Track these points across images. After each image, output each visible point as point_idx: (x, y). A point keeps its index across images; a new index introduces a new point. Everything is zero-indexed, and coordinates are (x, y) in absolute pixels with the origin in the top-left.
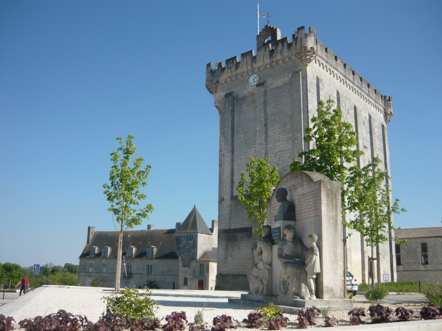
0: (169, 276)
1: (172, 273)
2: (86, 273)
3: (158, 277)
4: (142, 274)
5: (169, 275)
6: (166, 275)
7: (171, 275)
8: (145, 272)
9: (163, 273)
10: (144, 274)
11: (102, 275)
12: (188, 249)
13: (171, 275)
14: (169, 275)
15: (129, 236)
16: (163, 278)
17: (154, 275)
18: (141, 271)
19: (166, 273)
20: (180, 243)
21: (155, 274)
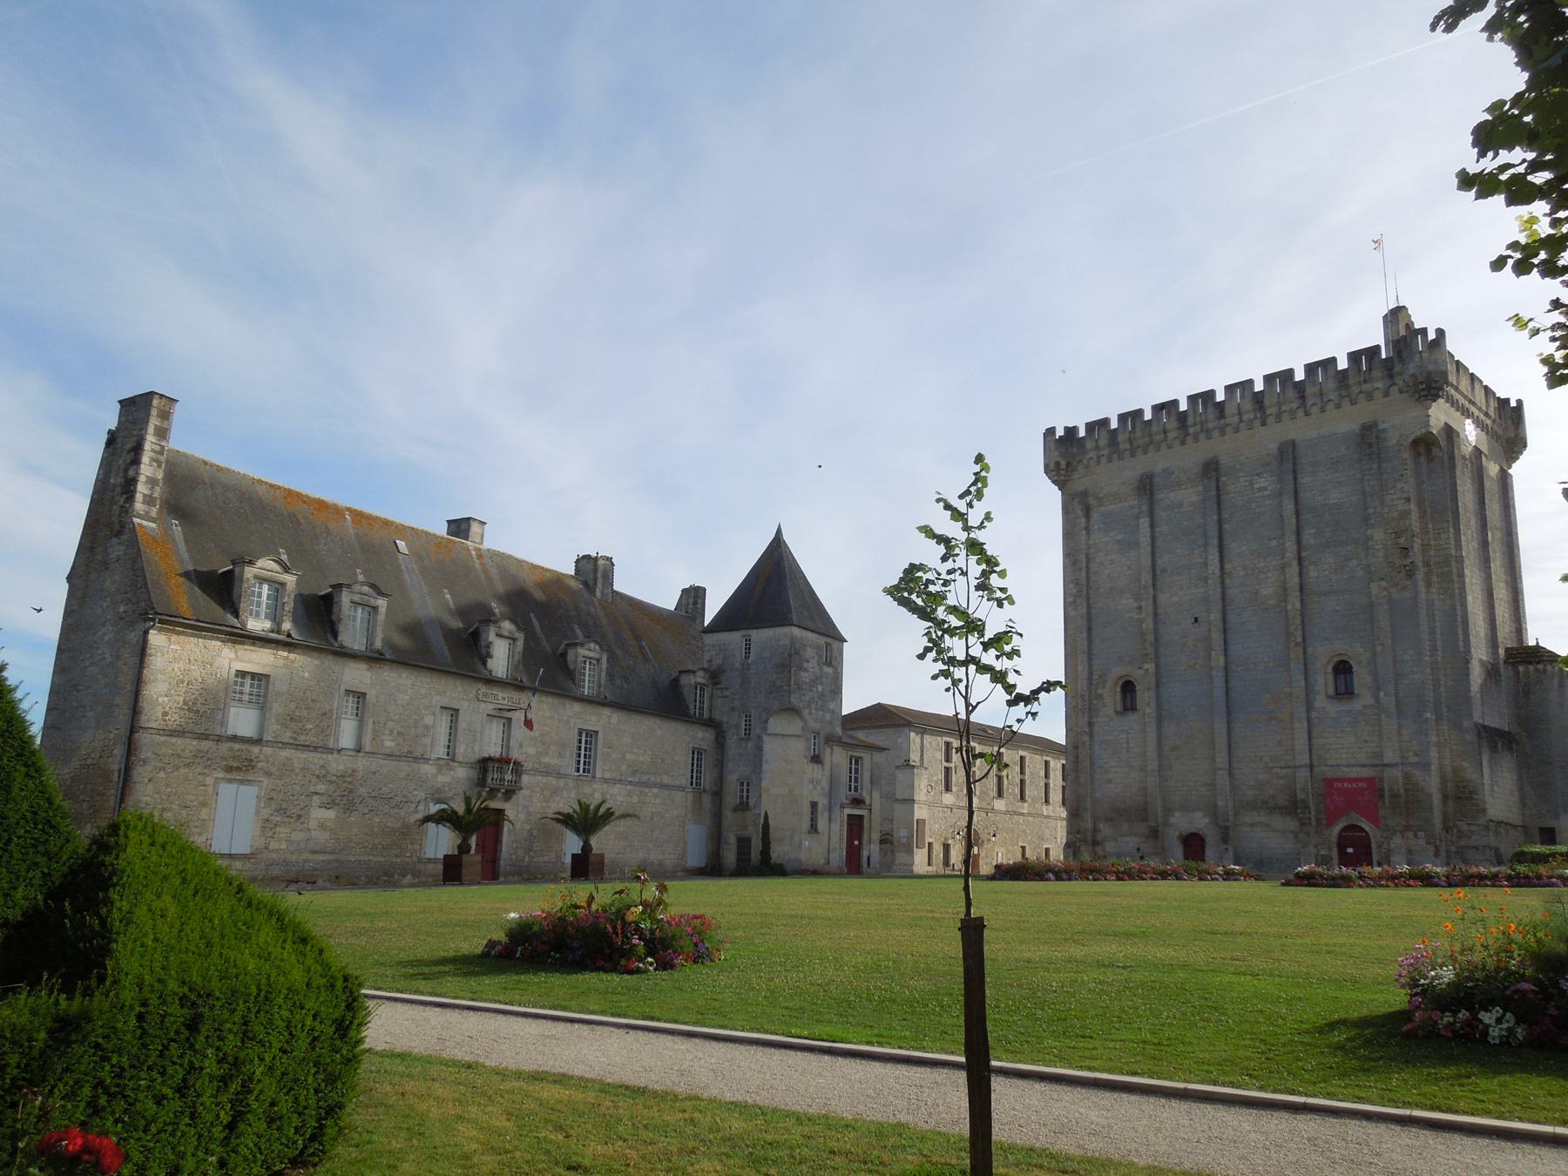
0: (655, 790)
1: (666, 780)
2: (205, 745)
3: (616, 789)
4: (559, 775)
5: (655, 785)
6: (646, 784)
7: (662, 786)
8: (568, 764)
9: (634, 773)
10: (565, 776)
11: (337, 764)
12: (822, 695)
13: (662, 786)
14: (655, 785)
15: (401, 544)
16: (635, 799)
17: (606, 781)
18: (551, 760)
19: (644, 778)
20: (800, 668)
21: (607, 775)
